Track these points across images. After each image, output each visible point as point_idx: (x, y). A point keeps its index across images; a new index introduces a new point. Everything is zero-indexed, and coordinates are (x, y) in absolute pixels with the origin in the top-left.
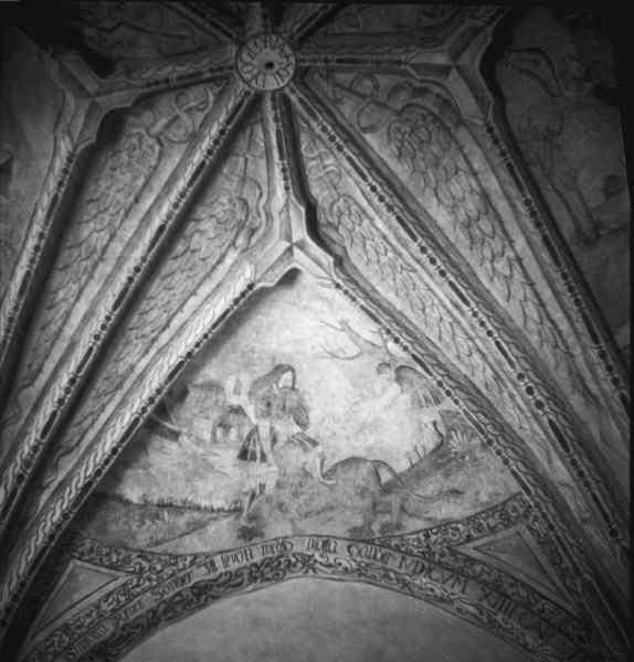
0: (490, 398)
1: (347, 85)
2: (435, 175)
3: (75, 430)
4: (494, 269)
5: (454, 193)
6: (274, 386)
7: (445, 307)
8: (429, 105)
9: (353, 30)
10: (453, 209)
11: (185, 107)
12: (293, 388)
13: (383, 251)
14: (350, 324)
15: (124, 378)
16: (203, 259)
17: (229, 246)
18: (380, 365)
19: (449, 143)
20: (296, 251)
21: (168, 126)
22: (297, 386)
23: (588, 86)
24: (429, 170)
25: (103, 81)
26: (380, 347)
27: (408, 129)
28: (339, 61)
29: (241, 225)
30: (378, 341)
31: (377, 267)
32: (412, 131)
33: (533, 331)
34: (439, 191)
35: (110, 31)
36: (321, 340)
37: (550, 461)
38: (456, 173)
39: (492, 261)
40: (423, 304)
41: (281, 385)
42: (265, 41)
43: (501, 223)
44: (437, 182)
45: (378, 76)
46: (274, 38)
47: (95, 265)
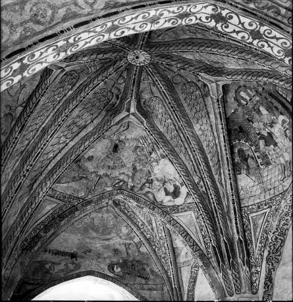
1: (122, 75)
7: (42, 124)
8: (112, 101)
9: (142, 78)
10: (79, 116)
18: (9, 105)
23: (117, 142)
24: (90, 104)
31: (53, 95)
38: (91, 114)
39: (63, 135)
40: (41, 116)
43: (77, 135)
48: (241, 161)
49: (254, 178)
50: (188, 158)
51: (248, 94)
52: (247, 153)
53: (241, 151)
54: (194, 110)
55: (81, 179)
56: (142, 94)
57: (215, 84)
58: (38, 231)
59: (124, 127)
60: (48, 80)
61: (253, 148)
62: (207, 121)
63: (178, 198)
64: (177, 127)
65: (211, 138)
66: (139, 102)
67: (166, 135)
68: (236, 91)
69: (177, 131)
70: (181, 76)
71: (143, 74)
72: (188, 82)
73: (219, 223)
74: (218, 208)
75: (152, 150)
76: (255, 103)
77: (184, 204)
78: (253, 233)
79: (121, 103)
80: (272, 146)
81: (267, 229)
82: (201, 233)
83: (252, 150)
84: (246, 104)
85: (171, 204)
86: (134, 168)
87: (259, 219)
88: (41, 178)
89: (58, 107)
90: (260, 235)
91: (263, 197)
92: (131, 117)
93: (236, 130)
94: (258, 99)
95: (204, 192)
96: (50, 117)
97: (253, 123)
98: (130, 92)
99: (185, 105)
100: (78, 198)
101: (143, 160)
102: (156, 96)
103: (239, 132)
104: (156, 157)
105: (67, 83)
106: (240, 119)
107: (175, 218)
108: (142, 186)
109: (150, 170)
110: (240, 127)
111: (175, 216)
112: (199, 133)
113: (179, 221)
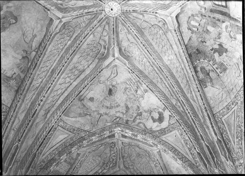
0: (30, 88)
1: (105, 28)
2: (85, 55)
4: (67, 78)
5: (82, 62)
6: (10, 18)
7: (51, 67)
8: (102, 50)
12: (10, 24)
13: (62, 45)
14: (36, 38)
18: (26, 50)
19: (93, 57)
20: (59, 20)
22: (11, 25)
23: (111, 87)
26: (31, 49)
27: (95, 46)
28: (113, 28)
30: (34, 48)
31: (57, 44)
32: (94, 47)
33: (54, 93)
34: (81, 57)
37: (22, 112)
38: (87, 61)
39: (68, 77)
40: (50, 60)
41: (10, 20)
42: (119, 9)
43: (78, 77)
44: (84, 56)
45: (108, 37)
46: (120, 12)
48: (204, 76)
49: (218, 87)
50: (164, 85)
51: (197, 21)
52: (207, 68)
53: (202, 69)
54: (161, 46)
55: (86, 116)
56: (122, 42)
57: (170, 17)
58: (53, 156)
59: (114, 74)
60: (51, 28)
61: (211, 63)
62: (172, 52)
63: (163, 122)
64: (151, 63)
65: (178, 65)
66: (120, 50)
67: (144, 71)
68: (188, 22)
69: (152, 66)
70: (146, 22)
71: (119, 26)
72: (152, 26)
73: (199, 132)
74: (196, 120)
75: (137, 88)
76: (203, 25)
77: (169, 126)
78: (229, 133)
79: (108, 49)
80: (224, 54)
81: (239, 123)
82: (187, 146)
83: (210, 65)
84: (198, 30)
85: (158, 129)
86: (127, 108)
87: (231, 119)
88: (53, 109)
89: (61, 54)
90: (235, 131)
91: (229, 99)
92: (116, 60)
93: (195, 52)
94: (204, 21)
95: (182, 111)
96: (56, 62)
97: (206, 43)
98: (112, 40)
99: (154, 44)
100: (85, 131)
101: (132, 98)
102: (132, 43)
103: (197, 54)
104: (141, 93)
105: (66, 35)
106: (195, 42)
107: (164, 139)
108: (134, 119)
109: (139, 106)
110: (197, 50)
111: (163, 138)
112: (168, 63)
113: (167, 141)
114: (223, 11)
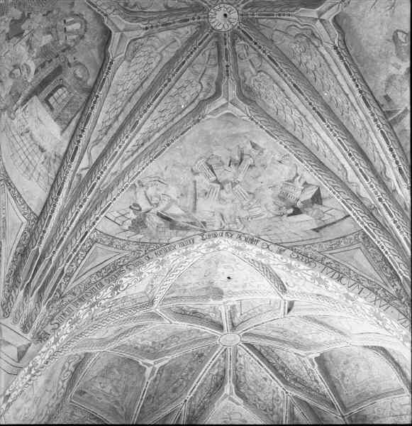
3: (377, 161)
11: (246, 55)
15: (364, 127)
16: (320, 66)
17: (318, 50)
21: (253, 66)
25: (222, 95)
29: (309, 40)
35: (202, 87)
36: (383, 10)
41: (404, 41)
42: (212, 18)
46: (210, 14)
47: (307, 120)
51: (72, 32)
57: (122, 29)
68: (86, 22)
76: (60, 33)
80: (8, 30)
84: (65, 21)
94: (61, 42)
97: (44, 15)
114: (46, 86)
